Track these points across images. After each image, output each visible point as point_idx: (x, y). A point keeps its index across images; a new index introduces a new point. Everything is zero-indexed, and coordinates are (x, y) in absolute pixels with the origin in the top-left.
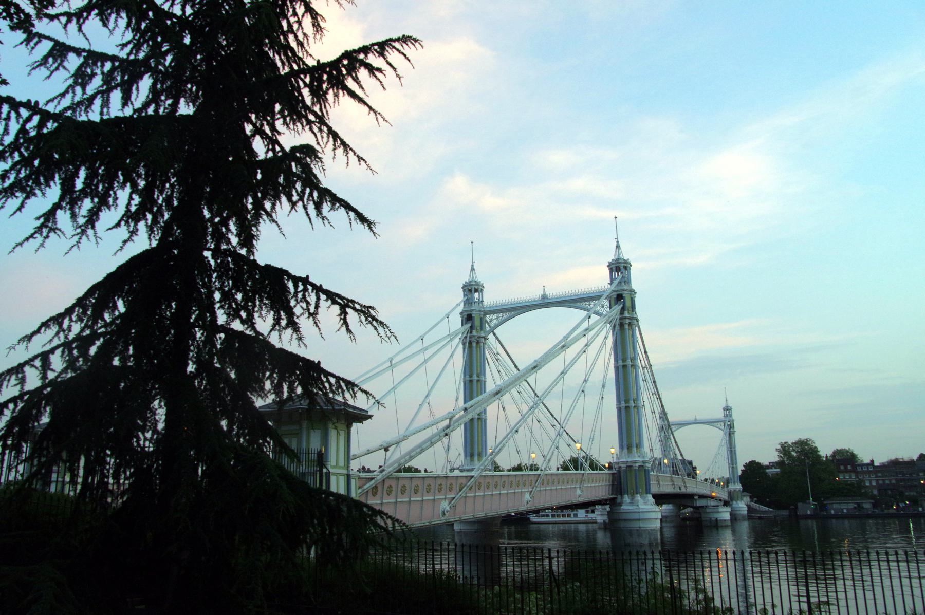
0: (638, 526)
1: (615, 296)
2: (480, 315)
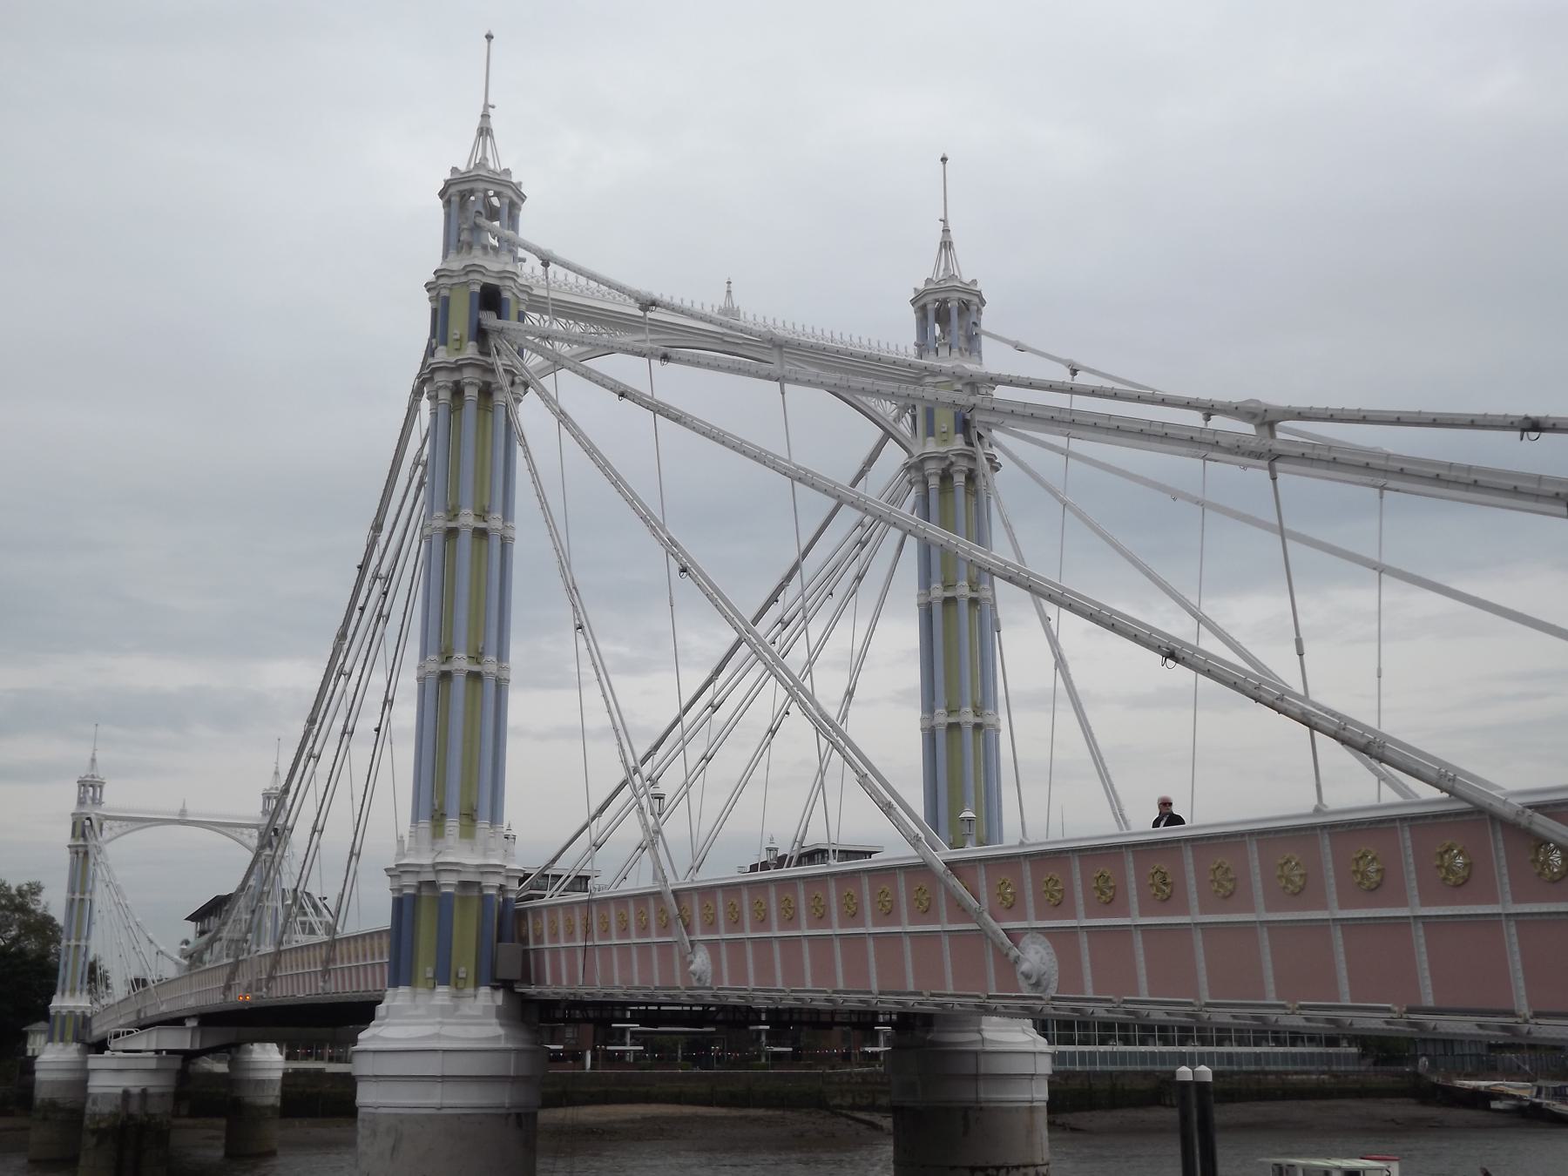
0: (1028, 1097)
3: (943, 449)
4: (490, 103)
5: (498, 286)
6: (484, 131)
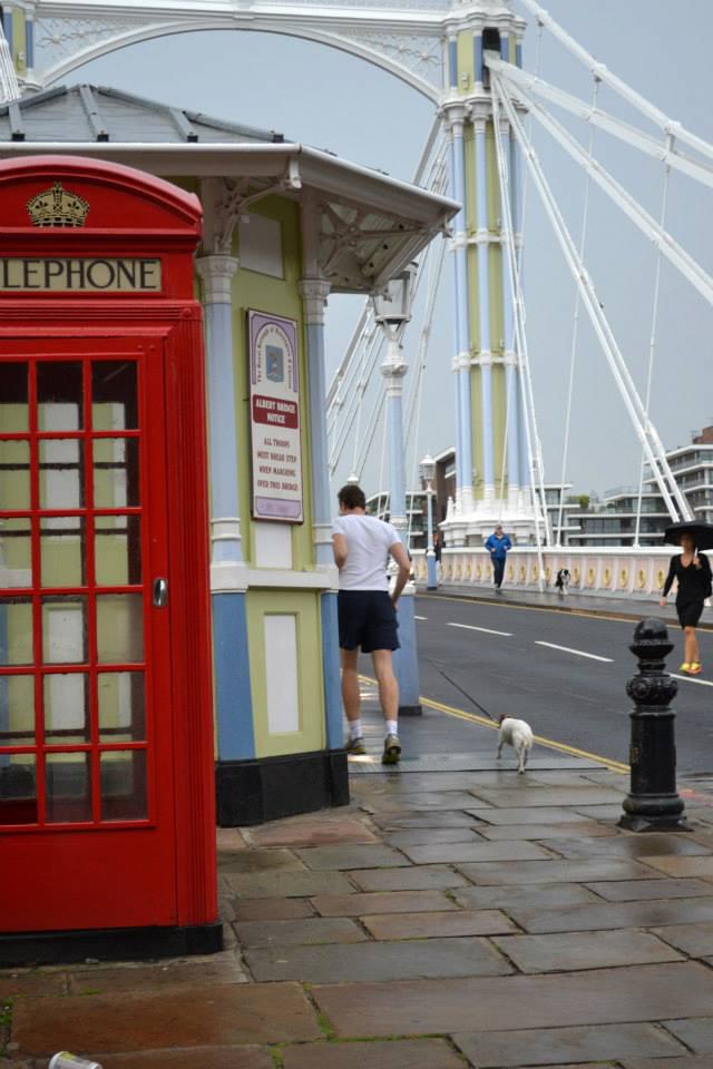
1: (479, 33)
3: (461, 99)
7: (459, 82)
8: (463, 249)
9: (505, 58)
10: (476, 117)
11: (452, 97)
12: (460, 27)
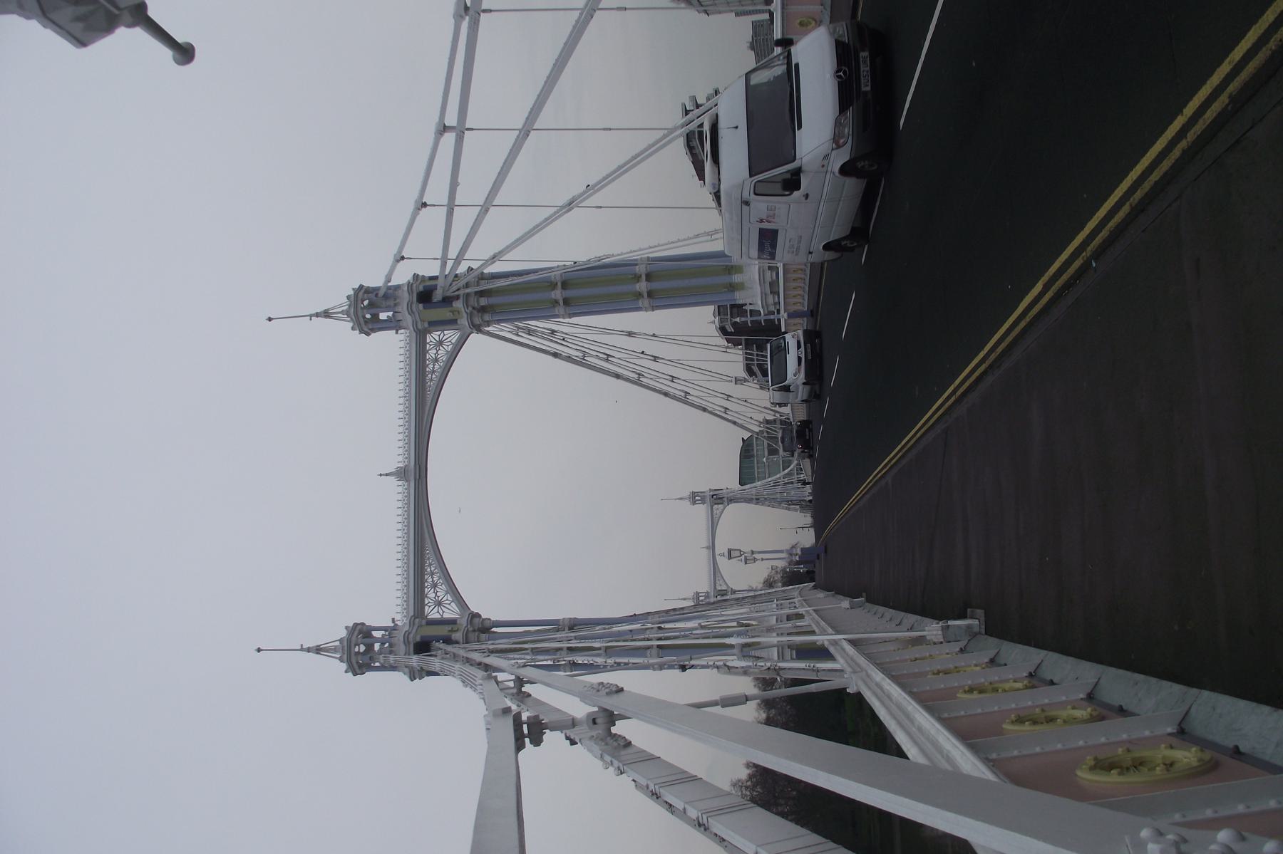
1: (421, 306)
2: (420, 626)
3: (465, 315)
4: (300, 648)
5: (414, 644)
6: (318, 650)
7: (454, 318)
8: (567, 308)
9: (435, 287)
10: (476, 305)
11: (464, 321)
12: (418, 320)
